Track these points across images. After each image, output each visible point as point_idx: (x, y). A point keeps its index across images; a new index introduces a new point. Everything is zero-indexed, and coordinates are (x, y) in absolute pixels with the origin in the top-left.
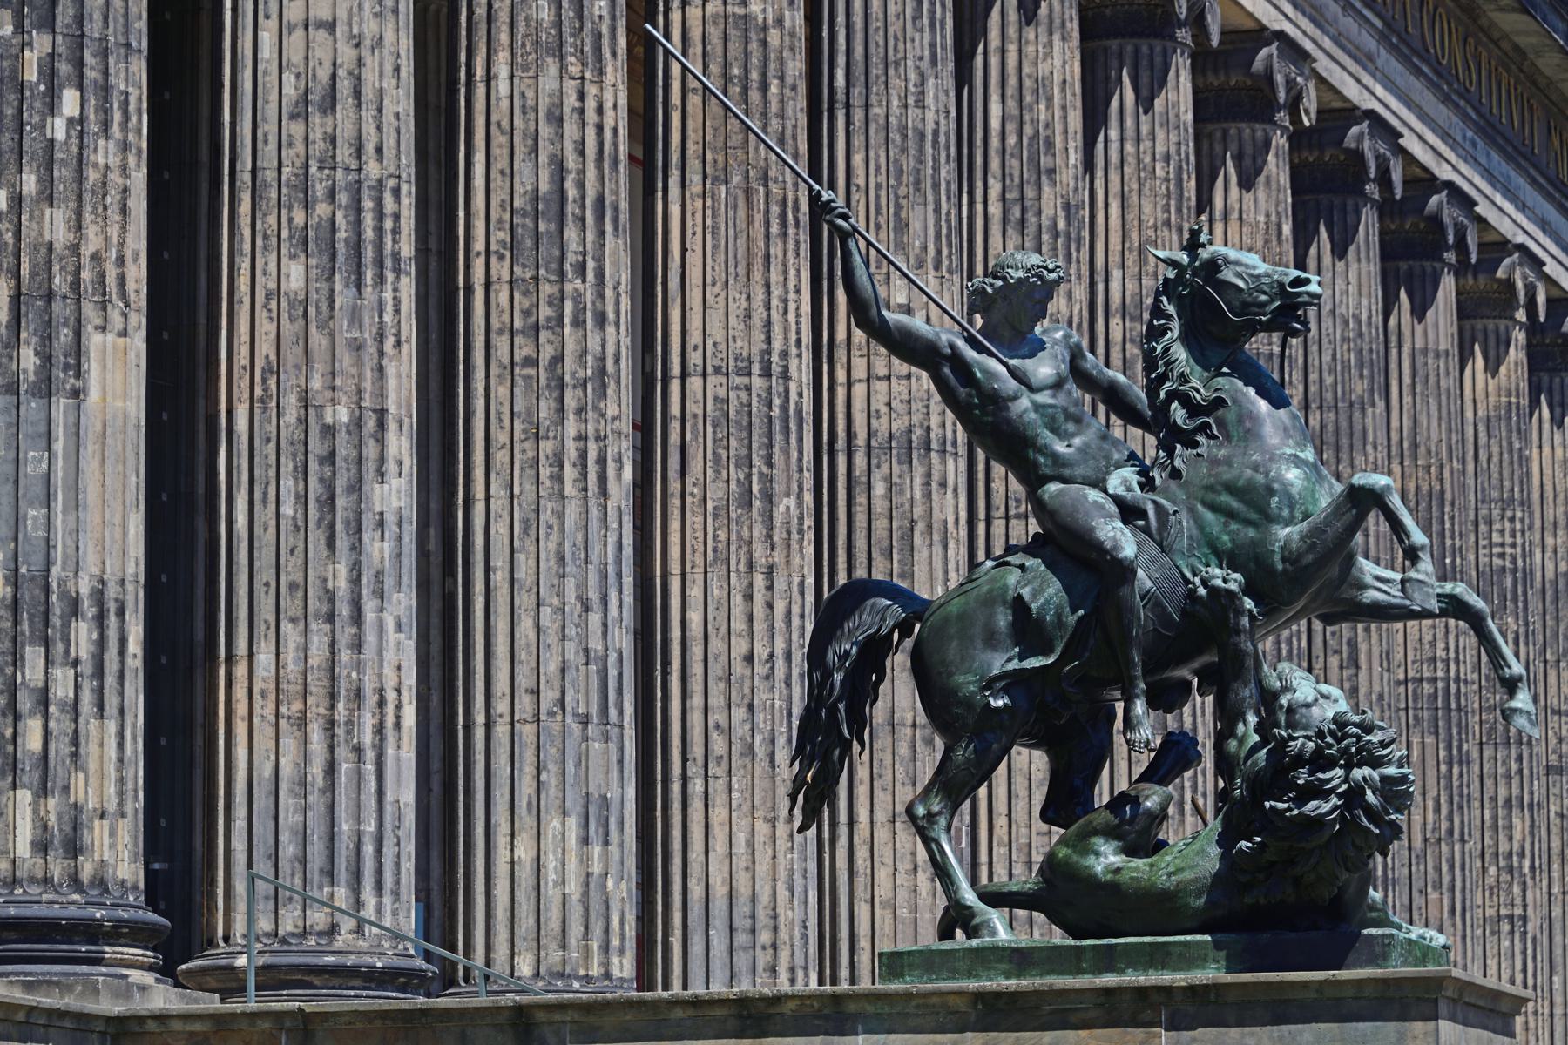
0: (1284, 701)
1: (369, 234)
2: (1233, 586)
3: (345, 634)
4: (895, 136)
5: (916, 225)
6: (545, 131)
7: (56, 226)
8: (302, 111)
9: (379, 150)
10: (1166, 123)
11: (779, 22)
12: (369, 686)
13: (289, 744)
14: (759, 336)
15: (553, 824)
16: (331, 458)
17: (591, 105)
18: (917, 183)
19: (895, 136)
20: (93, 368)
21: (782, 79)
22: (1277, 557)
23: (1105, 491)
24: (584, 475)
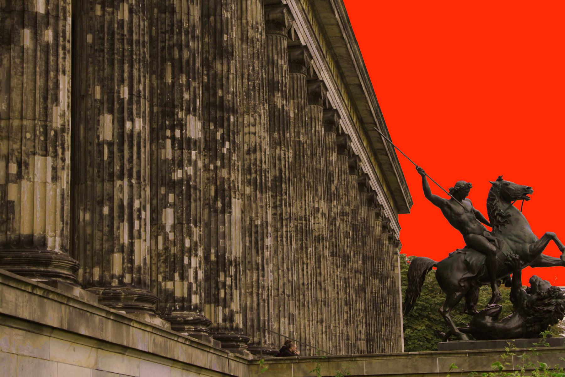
0: (537, 283)
1: (264, 181)
3: (261, 273)
4: (315, 170)
5: (319, 190)
6: (277, 162)
7: (224, 173)
8: (249, 153)
9: (265, 162)
10: (344, 173)
11: (306, 142)
12: (266, 285)
13: (249, 299)
14: (304, 212)
15: (282, 320)
16: (257, 232)
17: (287, 157)
18: (320, 181)
19: (315, 170)
20: (233, 206)
21: (307, 155)
22: (528, 251)
23: (483, 236)
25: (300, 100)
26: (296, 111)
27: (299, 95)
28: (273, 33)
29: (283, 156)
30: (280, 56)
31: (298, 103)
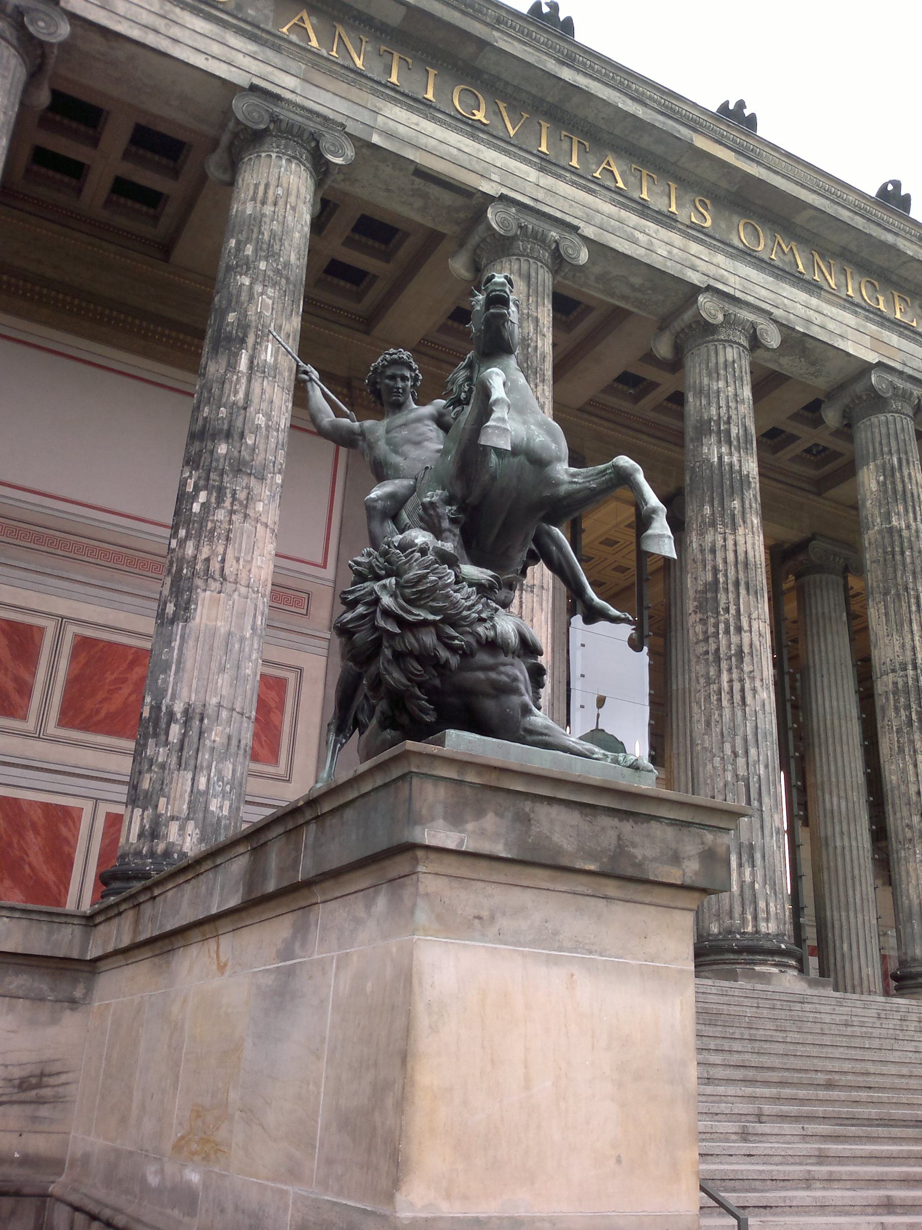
2: (435, 499)
6: (709, 557)
11: (908, 527)
14: (909, 653)
17: (730, 543)
21: (912, 549)
24: (732, 697)
25: (887, 457)
26: (882, 478)
27: (886, 449)
28: (700, 345)
29: (720, 542)
30: (715, 375)
31: (884, 466)
